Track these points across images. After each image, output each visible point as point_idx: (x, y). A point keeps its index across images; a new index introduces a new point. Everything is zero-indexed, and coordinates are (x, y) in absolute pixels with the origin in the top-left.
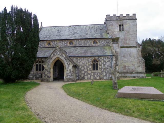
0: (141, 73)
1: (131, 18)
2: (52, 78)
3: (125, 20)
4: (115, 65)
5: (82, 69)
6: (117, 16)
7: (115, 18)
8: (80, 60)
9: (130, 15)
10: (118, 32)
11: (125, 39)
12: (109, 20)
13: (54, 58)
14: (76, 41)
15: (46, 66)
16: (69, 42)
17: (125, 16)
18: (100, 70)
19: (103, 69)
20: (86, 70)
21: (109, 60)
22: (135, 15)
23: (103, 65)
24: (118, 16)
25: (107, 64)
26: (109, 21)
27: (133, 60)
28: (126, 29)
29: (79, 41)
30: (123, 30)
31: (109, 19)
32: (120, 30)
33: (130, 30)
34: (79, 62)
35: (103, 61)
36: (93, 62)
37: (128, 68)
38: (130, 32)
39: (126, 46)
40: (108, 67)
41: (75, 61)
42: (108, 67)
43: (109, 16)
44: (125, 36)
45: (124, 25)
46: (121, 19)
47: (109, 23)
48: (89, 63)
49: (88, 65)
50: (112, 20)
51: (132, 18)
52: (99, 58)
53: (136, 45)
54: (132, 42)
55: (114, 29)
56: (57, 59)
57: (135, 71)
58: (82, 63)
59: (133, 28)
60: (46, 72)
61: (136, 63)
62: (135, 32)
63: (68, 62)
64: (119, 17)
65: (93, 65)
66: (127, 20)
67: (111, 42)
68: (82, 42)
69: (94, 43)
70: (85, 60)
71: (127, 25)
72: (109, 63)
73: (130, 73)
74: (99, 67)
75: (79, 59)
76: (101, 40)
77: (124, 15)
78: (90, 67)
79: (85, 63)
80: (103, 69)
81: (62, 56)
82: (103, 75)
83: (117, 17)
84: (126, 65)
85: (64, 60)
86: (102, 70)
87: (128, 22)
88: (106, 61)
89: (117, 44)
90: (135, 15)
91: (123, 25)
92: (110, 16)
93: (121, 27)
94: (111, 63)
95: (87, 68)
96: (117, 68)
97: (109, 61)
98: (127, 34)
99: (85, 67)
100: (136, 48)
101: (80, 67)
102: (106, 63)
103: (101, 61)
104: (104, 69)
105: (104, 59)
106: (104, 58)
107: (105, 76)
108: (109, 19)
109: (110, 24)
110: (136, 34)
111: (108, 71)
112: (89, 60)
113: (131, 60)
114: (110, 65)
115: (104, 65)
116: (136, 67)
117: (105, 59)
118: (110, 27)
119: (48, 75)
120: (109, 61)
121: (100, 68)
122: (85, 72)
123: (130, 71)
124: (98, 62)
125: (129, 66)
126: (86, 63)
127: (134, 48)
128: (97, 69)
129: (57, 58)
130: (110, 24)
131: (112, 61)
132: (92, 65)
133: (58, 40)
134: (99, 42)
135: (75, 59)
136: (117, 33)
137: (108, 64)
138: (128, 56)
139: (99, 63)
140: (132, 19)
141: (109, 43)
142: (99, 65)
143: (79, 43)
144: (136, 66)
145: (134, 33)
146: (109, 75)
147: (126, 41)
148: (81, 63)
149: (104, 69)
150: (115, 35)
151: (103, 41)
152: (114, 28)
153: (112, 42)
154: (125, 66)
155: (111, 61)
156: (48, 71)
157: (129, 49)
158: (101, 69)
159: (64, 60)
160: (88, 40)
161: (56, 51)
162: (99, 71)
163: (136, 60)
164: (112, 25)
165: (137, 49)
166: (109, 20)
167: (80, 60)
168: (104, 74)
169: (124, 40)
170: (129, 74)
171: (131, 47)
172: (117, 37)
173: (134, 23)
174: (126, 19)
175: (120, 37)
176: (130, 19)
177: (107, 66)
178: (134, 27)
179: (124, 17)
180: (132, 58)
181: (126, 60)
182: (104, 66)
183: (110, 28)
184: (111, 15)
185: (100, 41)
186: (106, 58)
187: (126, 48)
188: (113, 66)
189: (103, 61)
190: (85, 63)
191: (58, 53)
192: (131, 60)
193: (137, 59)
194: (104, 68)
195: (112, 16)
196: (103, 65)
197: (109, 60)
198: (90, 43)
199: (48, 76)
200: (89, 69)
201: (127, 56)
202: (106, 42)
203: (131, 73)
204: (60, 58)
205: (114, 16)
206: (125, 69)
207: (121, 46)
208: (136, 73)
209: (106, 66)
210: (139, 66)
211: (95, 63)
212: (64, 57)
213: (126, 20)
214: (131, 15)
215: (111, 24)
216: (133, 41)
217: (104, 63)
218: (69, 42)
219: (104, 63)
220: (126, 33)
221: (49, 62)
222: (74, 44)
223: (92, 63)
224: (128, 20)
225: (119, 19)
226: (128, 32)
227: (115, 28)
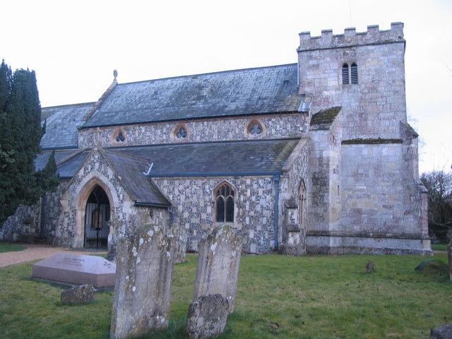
0: (413, 239)
1: (384, 38)
2: (79, 239)
3: (361, 46)
4: (285, 206)
5: (186, 215)
6: (335, 33)
7: (326, 42)
8: (181, 188)
9: (381, 29)
10: (339, 90)
11: (361, 115)
12: (306, 51)
13: (85, 180)
14: (194, 124)
15: (67, 204)
16: (173, 130)
17: (364, 34)
18: (239, 222)
19: (247, 219)
20: (194, 220)
21: (269, 186)
22: (398, 26)
23: (248, 203)
24: (337, 36)
25: (262, 202)
26: (308, 53)
27: (386, 190)
28: (367, 77)
29: (205, 123)
30: (355, 81)
31: (309, 46)
32: (345, 82)
33: (379, 81)
34: (176, 192)
35: (249, 191)
36: (218, 193)
37: (370, 220)
38: (381, 89)
39: (364, 137)
40: (265, 212)
41: (165, 192)
42: (265, 212)
43: (306, 37)
44: (361, 102)
45: (357, 64)
46: (348, 45)
47: (308, 61)
48: (207, 198)
49: (202, 204)
50: (317, 49)
51: (387, 39)
52: (239, 182)
53: (402, 135)
54: (387, 123)
55: (325, 79)
56: (92, 185)
57: (395, 231)
58: (187, 197)
59: (392, 72)
60: (66, 220)
61: (398, 200)
62: (398, 89)
63: (120, 192)
64: (341, 37)
65: (218, 204)
66: (370, 48)
67: (307, 125)
68: (214, 127)
69: (250, 129)
70: (195, 187)
71: (371, 63)
72: (269, 197)
73: (373, 237)
74: (236, 210)
75: (177, 182)
76: (273, 120)
77: (358, 31)
78: (209, 210)
79: (195, 197)
80: (247, 219)
81: (105, 174)
82: (248, 238)
83: (334, 37)
84: (362, 205)
85: (110, 185)
86: (244, 220)
87: (373, 51)
88: (261, 191)
89: (326, 133)
90: (398, 26)
91: (354, 65)
92: (313, 35)
93: (350, 72)
94: (276, 198)
95: (199, 215)
96: (295, 217)
97: (270, 192)
98: (370, 94)
99: (194, 210)
100: (399, 145)
101: (180, 208)
102: (258, 198)
103: (243, 192)
104: (251, 217)
105: (252, 185)
106: (252, 180)
107: (253, 241)
108: (308, 48)
109: (311, 62)
110: (400, 93)
111: (264, 226)
112: (207, 187)
113: (378, 189)
114: (271, 206)
115: (252, 204)
116: (399, 215)
117: (255, 186)
118: (311, 72)
119: (70, 228)
120: (270, 192)
121: (238, 213)
122: (192, 225)
123: (375, 229)
124: (233, 193)
125: (371, 213)
126: (198, 198)
127: (391, 145)
128: (230, 219)
129: (93, 179)
130: (311, 62)
131: (278, 191)
132: (213, 203)
133: (98, 128)
134: (267, 127)
135: (165, 182)
136: (333, 93)
137: (266, 201)
138: (371, 172)
139: (236, 198)
140: (386, 43)
141: (301, 129)
142: (235, 205)
143: (203, 132)
144: (398, 211)
145: (396, 92)
146: (268, 241)
147: (366, 120)
148: (183, 198)
149: (251, 217)
150: (326, 99)
151: (282, 122)
152: (322, 76)
153: (311, 124)
154: (358, 212)
155: (274, 193)
156: (71, 216)
157: (375, 149)
158: (242, 217)
159: (110, 185)
160: (232, 122)
161: (92, 159)
162: (236, 224)
163: (400, 188)
164: (317, 66)
165: (402, 149)
166: (306, 51)
167: (181, 188)
168: (252, 235)
169: (357, 118)
170: (373, 240)
171: (381, 141)
172: (334, 106)
173: (394, 57)
174: (368, 42)
175: (344, 106)
176: (379, 44)
177: (262, 207)
178: (394, 69)
179: (359, 37)
180: (383, 181)
181: (360, 190)
182: (251, 209)
183: (308, 77)
184: (316, 33)
185: (270, 123)
186: (260, 181)
187: (363, 146)
188: (280, 208)
189: (249, 191)
190: (195, 197)
191: (97, 165)
192: (378, 189)
193: (403, 186)
194: (252, 213)
195: (319, 34)
196: (248, 203)
197: (269, 186)
198: (237, 132)
199: (70, 233)
200: (204, 216)
201: (367, 176)
202: (289, 126)
203: (379, 236)
204: (99, 180)
205: (324, 35)
206: (358, 222)
207: (347, 139)
208: (395, 237)
209: (258, 208)
210: (407, 213)
211: (225, 199)
212: (111, 177)
213: (364, 48)
214: (385, 26)
215: (315, 62)
216: (389, 119)
217: (253, 198)
218: (176, 130)
219: (253, 198)
220: (366, 91)
221: (74, 191)
222: (189, 134)
223: (213, 198)
224: (373, 44)
225: (340, 45)
226: (374, 89)
227: (326, 76)
